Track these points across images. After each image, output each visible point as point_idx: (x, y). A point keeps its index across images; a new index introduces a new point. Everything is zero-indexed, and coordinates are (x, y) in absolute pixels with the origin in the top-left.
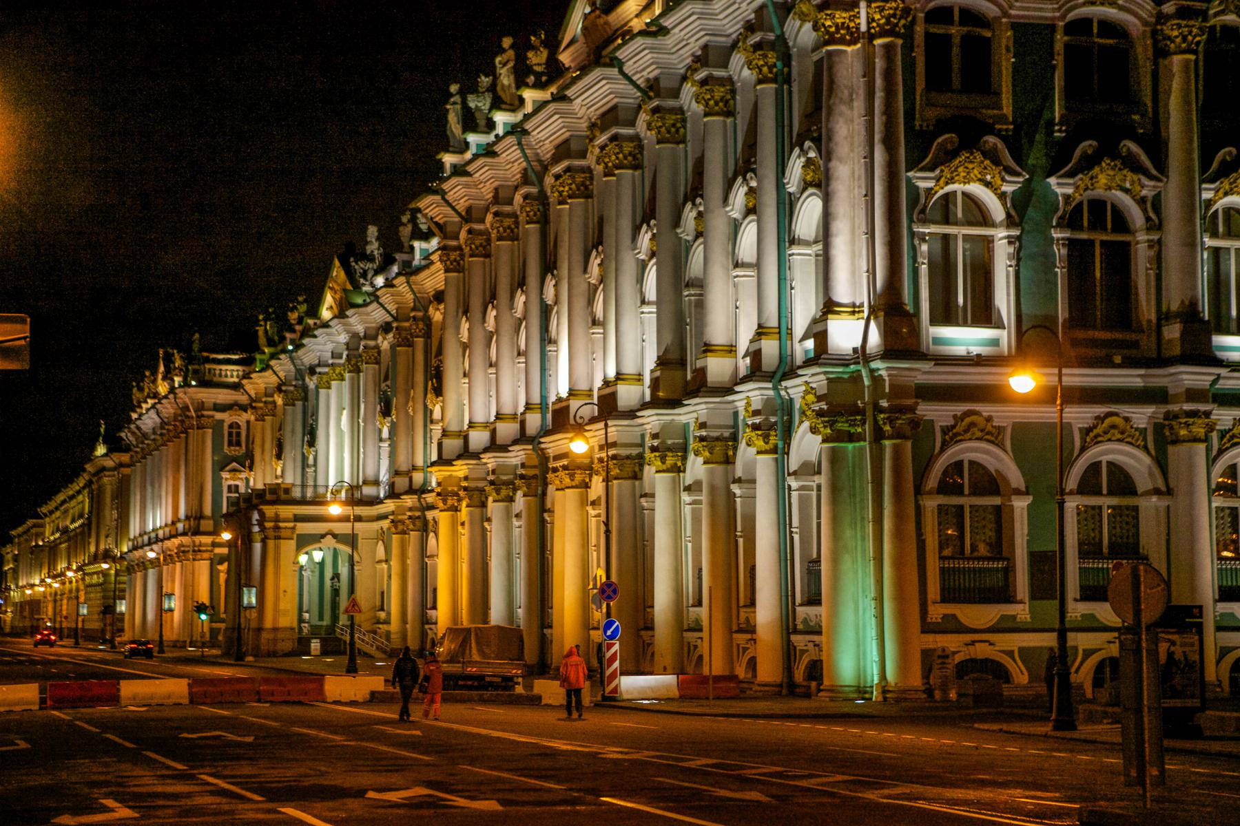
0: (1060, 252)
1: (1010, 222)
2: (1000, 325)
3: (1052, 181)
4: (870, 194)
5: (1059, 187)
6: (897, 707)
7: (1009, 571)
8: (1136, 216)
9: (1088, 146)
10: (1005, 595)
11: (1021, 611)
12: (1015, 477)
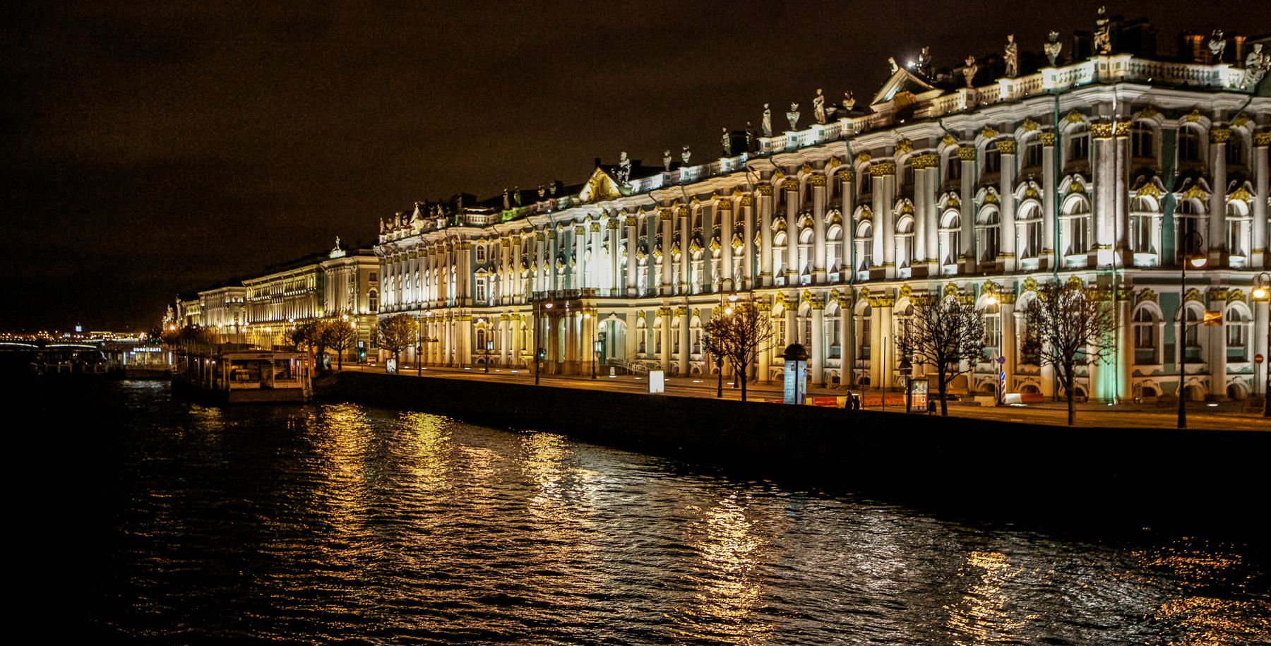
0: (1176, 223)
1: (1160, 211)
2: (1153, 252)
3: (1175, 195)
4: (1115, 200)
5: (1177, 197)
6: (1125, 405)
7: (1156, 352)
8: (1201, 207)
9: (1188, 180)
10: (1154, 361)
11: (1160, 368)
12: (1160, 315)
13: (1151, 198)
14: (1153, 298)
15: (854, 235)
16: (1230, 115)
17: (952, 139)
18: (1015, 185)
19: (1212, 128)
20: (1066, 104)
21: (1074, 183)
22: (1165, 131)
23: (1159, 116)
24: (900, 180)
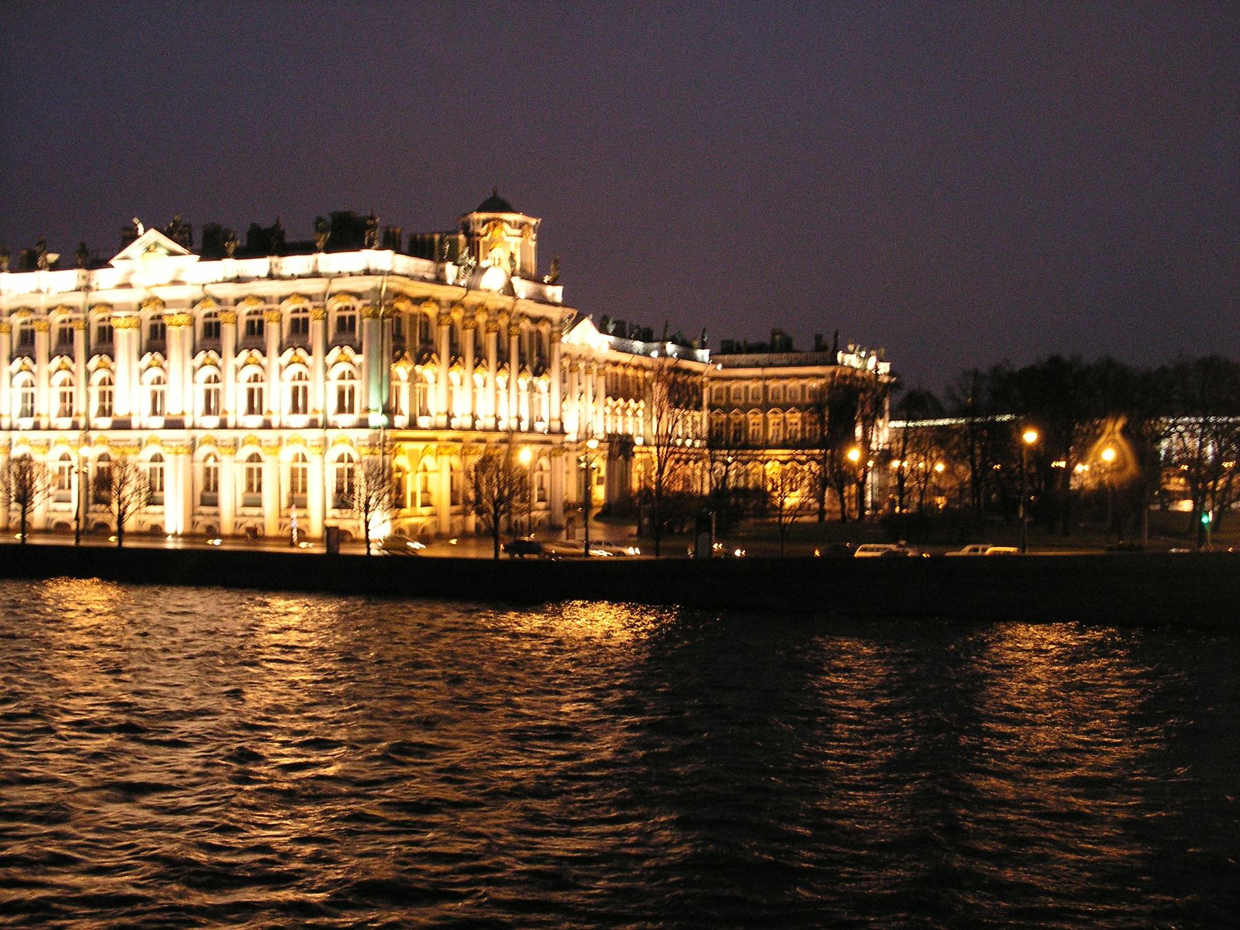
13: (402, 370)
14: (404, 453)
15: (88, 384)
16: (453, 304)
17: (211, 302)
18: (281, 351)
19: (439, 314)
20: (337, 285)
21: (342, 353)
22: (413, 316)
23: (408, 303)
24: (146, 335)
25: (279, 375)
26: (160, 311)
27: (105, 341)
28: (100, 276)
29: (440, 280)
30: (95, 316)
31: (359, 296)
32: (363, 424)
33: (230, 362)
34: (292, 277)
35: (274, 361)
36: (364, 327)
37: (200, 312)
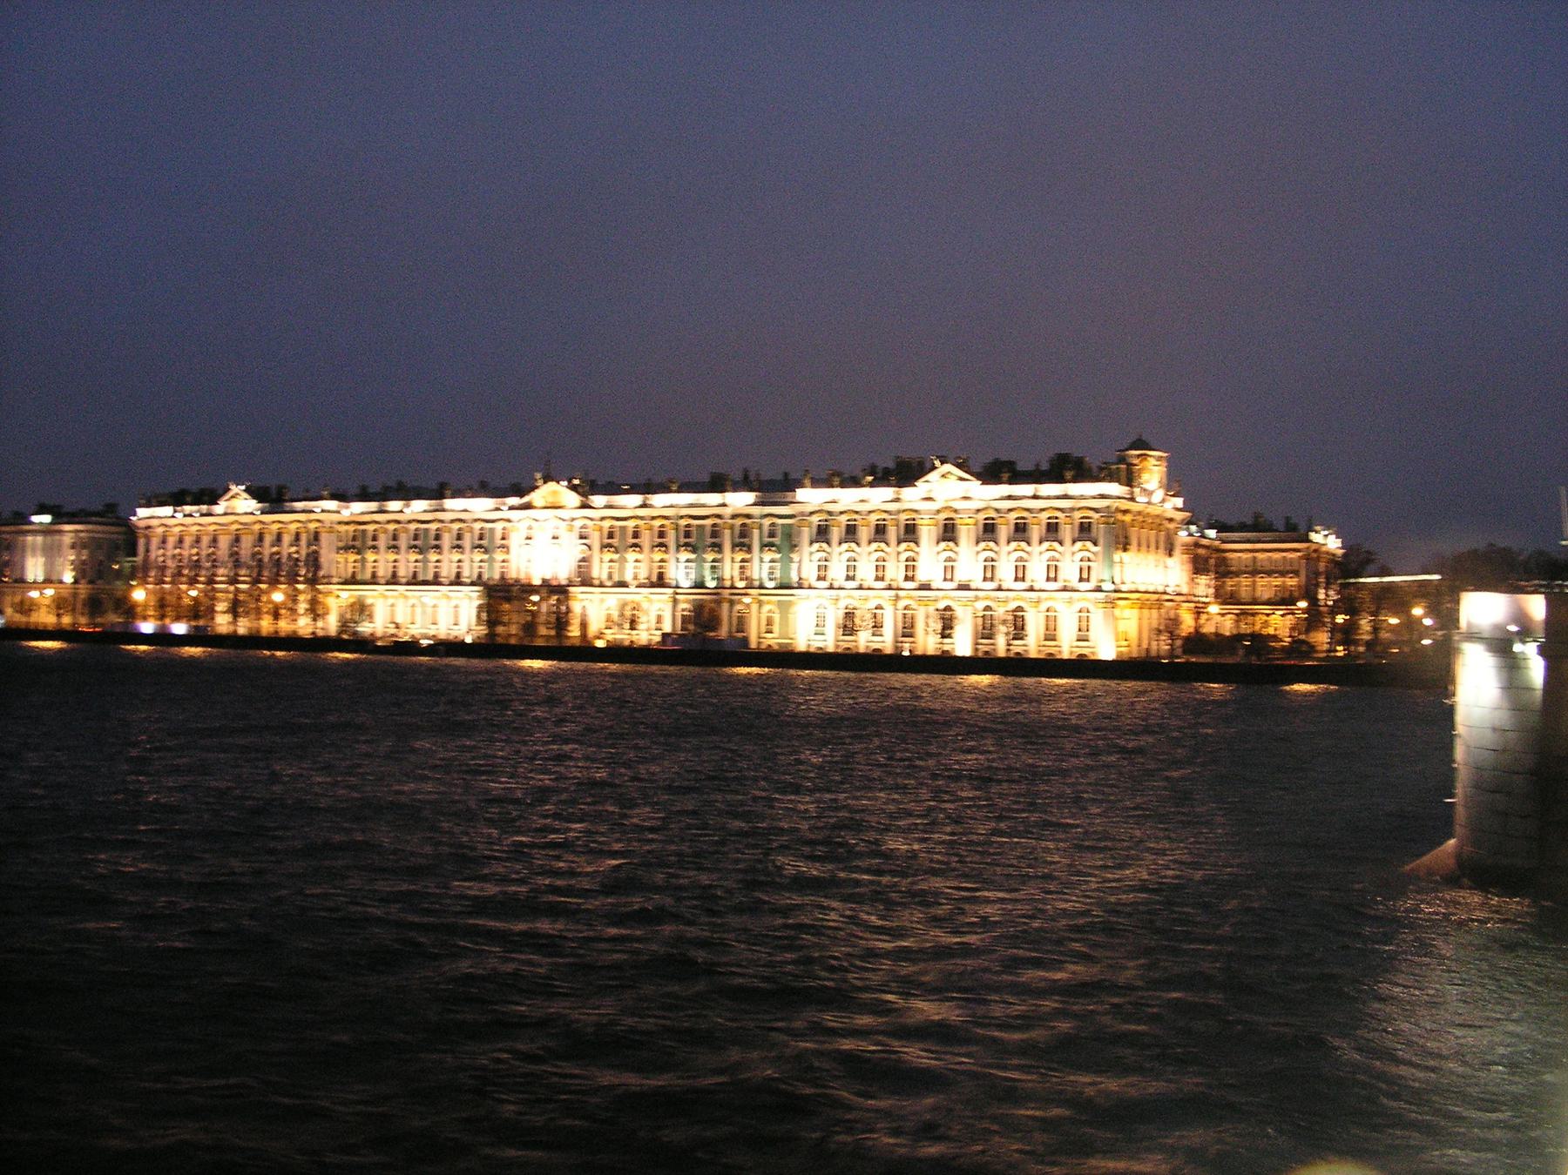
16: (1139, 513)
25: (1038, 557)
26: (953, 515)
27: (910, 532)
28: (907, 493)
29: (1132, 499)
30: (903, 517)
31: (1096, 510)
32: (1098, 589)
33: (1005, 548)
34: (1048, 498)
35: (1036, 548)
36: (1100, 531)
37: (982, 516)
